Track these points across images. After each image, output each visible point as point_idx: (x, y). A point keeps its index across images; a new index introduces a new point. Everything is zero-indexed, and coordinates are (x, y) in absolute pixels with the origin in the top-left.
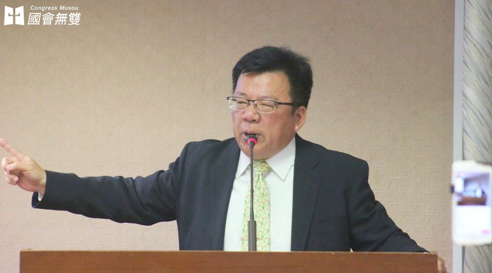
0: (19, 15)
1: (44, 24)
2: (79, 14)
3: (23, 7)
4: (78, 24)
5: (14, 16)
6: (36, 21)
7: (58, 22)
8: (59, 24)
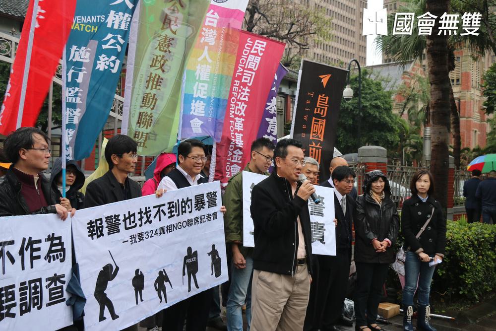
2: (479, 15)
4: (477, 34)
6: (406, 28)
7: (443, 30)
8: (445, 34)
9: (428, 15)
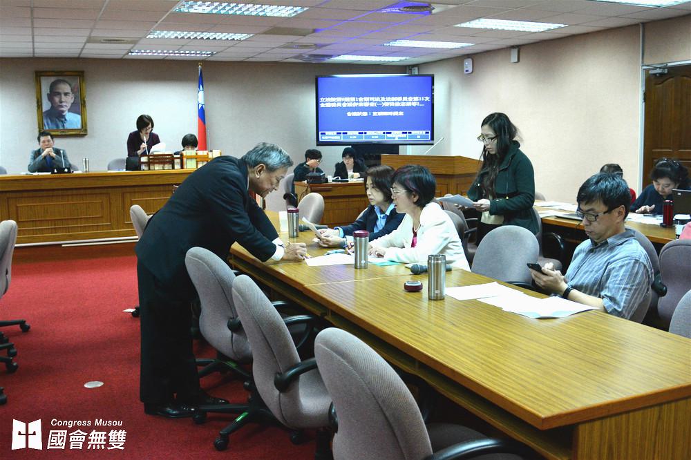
0: (34, 434)
1: (71, 448)
3: (39, 422)
4: (122, 448)
5: (27, 435)
6: (59, 443)
7: (92, 445)
9: (78, 433)
